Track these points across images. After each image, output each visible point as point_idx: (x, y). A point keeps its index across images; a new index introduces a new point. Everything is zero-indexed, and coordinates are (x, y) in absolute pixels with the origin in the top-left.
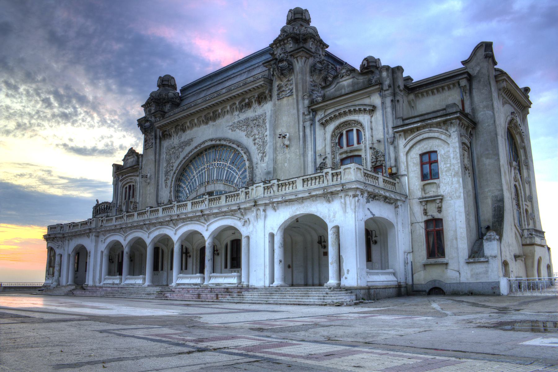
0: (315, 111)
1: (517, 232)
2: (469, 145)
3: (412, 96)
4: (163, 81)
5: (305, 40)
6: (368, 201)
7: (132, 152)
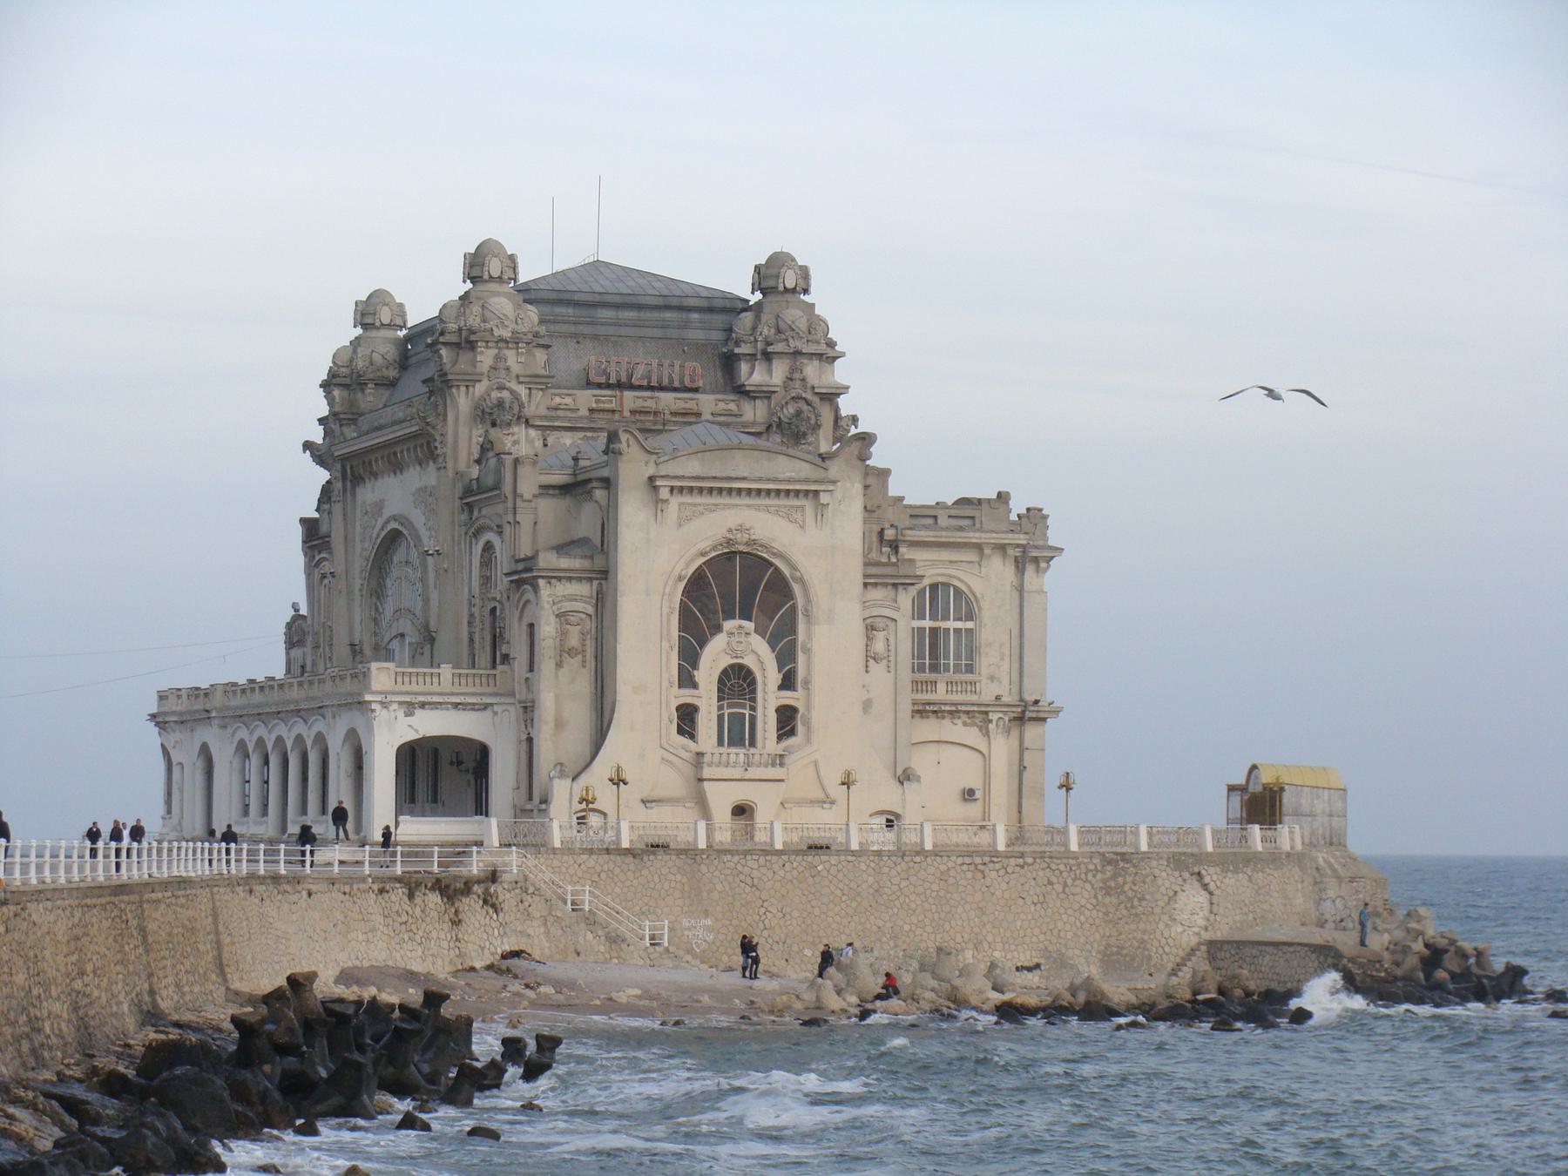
0: (470, 506)
1: (671, 758)
2: (590, 610)
3: (565, 502)
4: (363, 315)
5: (472, 345)
6: (409, 714)
7: (326, 493)
